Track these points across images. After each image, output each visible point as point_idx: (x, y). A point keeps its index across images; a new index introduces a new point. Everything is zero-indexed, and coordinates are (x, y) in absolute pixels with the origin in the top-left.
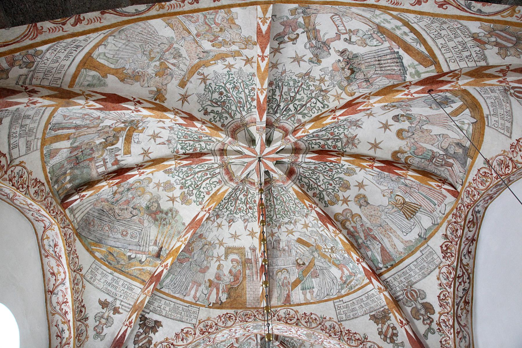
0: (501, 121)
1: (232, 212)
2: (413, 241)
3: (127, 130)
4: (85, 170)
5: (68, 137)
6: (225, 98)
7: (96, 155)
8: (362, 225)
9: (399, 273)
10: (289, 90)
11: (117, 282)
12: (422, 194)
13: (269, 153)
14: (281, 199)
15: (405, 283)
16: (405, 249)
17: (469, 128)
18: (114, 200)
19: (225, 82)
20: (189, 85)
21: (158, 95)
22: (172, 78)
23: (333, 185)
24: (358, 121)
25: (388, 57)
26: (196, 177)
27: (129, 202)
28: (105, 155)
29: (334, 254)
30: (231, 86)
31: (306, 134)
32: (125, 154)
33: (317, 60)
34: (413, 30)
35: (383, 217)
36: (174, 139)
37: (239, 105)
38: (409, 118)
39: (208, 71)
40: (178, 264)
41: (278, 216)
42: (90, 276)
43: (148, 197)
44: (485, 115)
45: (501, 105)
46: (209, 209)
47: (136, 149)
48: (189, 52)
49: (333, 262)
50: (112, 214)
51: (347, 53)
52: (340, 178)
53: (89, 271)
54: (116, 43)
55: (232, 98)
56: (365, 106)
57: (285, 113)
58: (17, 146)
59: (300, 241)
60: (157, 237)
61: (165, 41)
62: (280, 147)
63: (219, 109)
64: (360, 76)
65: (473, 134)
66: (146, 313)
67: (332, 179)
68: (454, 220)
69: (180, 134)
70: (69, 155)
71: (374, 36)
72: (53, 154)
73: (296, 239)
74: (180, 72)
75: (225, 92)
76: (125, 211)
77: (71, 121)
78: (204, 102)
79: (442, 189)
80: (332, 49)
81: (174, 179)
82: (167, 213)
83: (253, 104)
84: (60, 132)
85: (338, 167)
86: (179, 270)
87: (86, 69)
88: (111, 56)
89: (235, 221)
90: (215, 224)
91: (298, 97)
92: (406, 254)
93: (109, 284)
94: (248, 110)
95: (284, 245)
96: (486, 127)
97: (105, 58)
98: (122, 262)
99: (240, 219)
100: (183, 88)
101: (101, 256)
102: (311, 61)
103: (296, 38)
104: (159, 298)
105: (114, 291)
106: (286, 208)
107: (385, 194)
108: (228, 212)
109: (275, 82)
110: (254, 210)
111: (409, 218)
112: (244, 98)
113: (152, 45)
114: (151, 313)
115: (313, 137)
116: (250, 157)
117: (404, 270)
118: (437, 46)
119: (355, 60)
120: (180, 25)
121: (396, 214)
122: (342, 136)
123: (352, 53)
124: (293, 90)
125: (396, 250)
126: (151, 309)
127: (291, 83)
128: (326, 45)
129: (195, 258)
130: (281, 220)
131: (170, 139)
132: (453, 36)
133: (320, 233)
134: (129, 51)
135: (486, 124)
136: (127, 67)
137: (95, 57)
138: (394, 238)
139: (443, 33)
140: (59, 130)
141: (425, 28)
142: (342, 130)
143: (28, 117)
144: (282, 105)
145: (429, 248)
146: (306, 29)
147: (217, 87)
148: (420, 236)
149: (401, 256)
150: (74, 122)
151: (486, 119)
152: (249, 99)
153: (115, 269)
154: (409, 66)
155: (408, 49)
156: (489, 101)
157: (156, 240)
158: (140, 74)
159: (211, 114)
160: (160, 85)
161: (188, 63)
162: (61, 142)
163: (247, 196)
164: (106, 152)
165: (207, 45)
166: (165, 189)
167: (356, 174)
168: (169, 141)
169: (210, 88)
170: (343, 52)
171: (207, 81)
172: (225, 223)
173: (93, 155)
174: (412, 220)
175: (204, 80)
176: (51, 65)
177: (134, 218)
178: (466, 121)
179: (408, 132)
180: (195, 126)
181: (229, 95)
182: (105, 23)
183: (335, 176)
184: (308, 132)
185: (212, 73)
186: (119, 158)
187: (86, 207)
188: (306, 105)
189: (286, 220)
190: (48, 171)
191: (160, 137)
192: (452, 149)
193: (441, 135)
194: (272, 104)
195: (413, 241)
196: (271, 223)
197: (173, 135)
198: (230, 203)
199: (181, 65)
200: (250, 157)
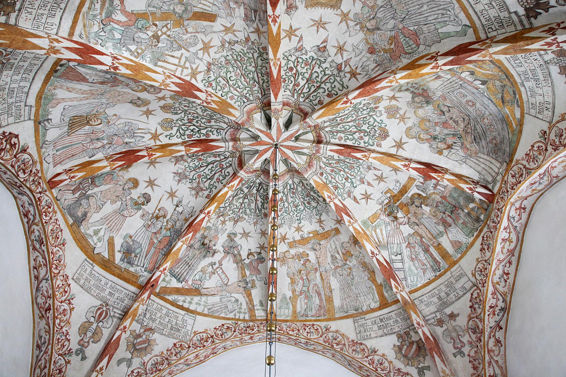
0: (85, 275)
1: (318, 62)
2: (50, 110)
3: (400, 202)
4: (455, 195)
5: (439, 247)
7: (438, 198)
8: (127, 85)
9: (36, 68)
10: (249, 205)
11: (525, 73)
12: (77, 144)
13: (266, 151)
14: (248, 80)
15: (16, 62)
16: (53, 95)
17: (93, 240)
18: (456, 140)
20: (334, 227)
22: (343, 243)
23: (182, 106)
24: (179, 181)
25: (185, 274)
26: (355, 117)
27: (444, 123)
28: (432, 191)
29: (150, 34)
30: (299, 207)
31: (230, 185)
32: (415, 180)
33: (231, 237)
34: (181, 308)
35: (104, 100)
38: (137, 205)
39: (315, 227)
40: (422, 37)
41: (251, 56)
42: (546, 112)
43: (420, 112)
44: (94, 264)
45: (97, 287)
46: (346, 102)
47: (403, 178)
49: (147, 19)
50: (469, 126)
51: (211, 255)
52: (176, 114)
53: (540, 116)
55: (300, 197)
56: (188, 238)
57: (251, 184)
58: (463, 287)
59: (211, 17)
60: (433, 80)
61: (338, 276)
62: (255, 161)
63: (312, 193)
64: (197, 245)
65: (86, 240)
66: (519, 17)
67: (186, 111)
68: (34, 171)
69: (356, 171)
70: (453, 225)
71: (199, 282)
72: (457, 245)
73: (219, 19)
76: (454, 117)
77: (425, 262)
79: (68, 178)
80: (222, 251)
81: (381, 118)
82: (407, 90)
83: (282, 194)
84: (439, 258)
85: (183, 127)
86: (425, 28)
88: (371, 294)
89: (316, 48)
90: (346, 56)
91: (241, 200)
92: (46, 90)
93: (537, 80)
94: (286, 186)
95: (237, 10)
96: (86, 257)
98: (498, 83)
99: (308, 49)
101: (516, 108)
102: (235, 234)
103: (249, 255)
104: (482, 18)
105: (538, 70)
106: (240, 65)
107: (115, 117)
108: (324, 66)
110: (285, 68)
111: (72, 118)
112: (289, 197)
114: (512, 10)
115: (219, 155)
116: (287, 147)
117: (32, 74)
118: (164, 307)
119: (204, 253)
121: (88, 110)
122: (189, 160)
123: (208, 257)
124: (246, 204)
125: (65, 88)
126: (506, 14)
127: (248, 211)
128: (227, 253)
129: (392, 23)
130: (245, 49)
131: (367, 170)
132: (162, 321)
133: (183, 51)
135: (88, 259)
136: (366, 278)
138: (77, 96)
139: (167, 319)
140: (437, 261)
141: (178, 315)
142: (191, 165)
143: (440, 298)
144: (254, 191)
145: (26, 119)
146: (243, 263)
148: (48, 120)
149: (51, 85)
150: (424, 258)
151: (92, 262)
152: (284, 198)
153: (514, 84)
154: (171, 280)
155: (178, 291)
156: (104, 280)
157: (436, 78)
161: (329, 246)
162: (445, 247)
163: (294, 85)
164: (429, 193)
165: (312, 256)
166: (398, 109)
167: (159, 124)
168: (369, 168)
170: (215, 253)
172: (332, 51)
173: (440, 199)
174: (69, 119)
175: (320, 221)
176: (400, 321)
177: (449, 105)
178: (99, 245)
179: (129, 188)
180: (336, 205)
181: (302, 200)
182: (351, 359)
183: (183, 115)
184: (228, 188)
185: (313, 224)
186: (422, 180)
187: (484, 161)
188: (233, 198)
189: (238, 47)
190: (472, 238)
191: (376, 175)
192: (85, 204)
193: (101, 206)
195: (50, 110)
196: (261, 50)
198: (319, 80)
200: (287, 147)
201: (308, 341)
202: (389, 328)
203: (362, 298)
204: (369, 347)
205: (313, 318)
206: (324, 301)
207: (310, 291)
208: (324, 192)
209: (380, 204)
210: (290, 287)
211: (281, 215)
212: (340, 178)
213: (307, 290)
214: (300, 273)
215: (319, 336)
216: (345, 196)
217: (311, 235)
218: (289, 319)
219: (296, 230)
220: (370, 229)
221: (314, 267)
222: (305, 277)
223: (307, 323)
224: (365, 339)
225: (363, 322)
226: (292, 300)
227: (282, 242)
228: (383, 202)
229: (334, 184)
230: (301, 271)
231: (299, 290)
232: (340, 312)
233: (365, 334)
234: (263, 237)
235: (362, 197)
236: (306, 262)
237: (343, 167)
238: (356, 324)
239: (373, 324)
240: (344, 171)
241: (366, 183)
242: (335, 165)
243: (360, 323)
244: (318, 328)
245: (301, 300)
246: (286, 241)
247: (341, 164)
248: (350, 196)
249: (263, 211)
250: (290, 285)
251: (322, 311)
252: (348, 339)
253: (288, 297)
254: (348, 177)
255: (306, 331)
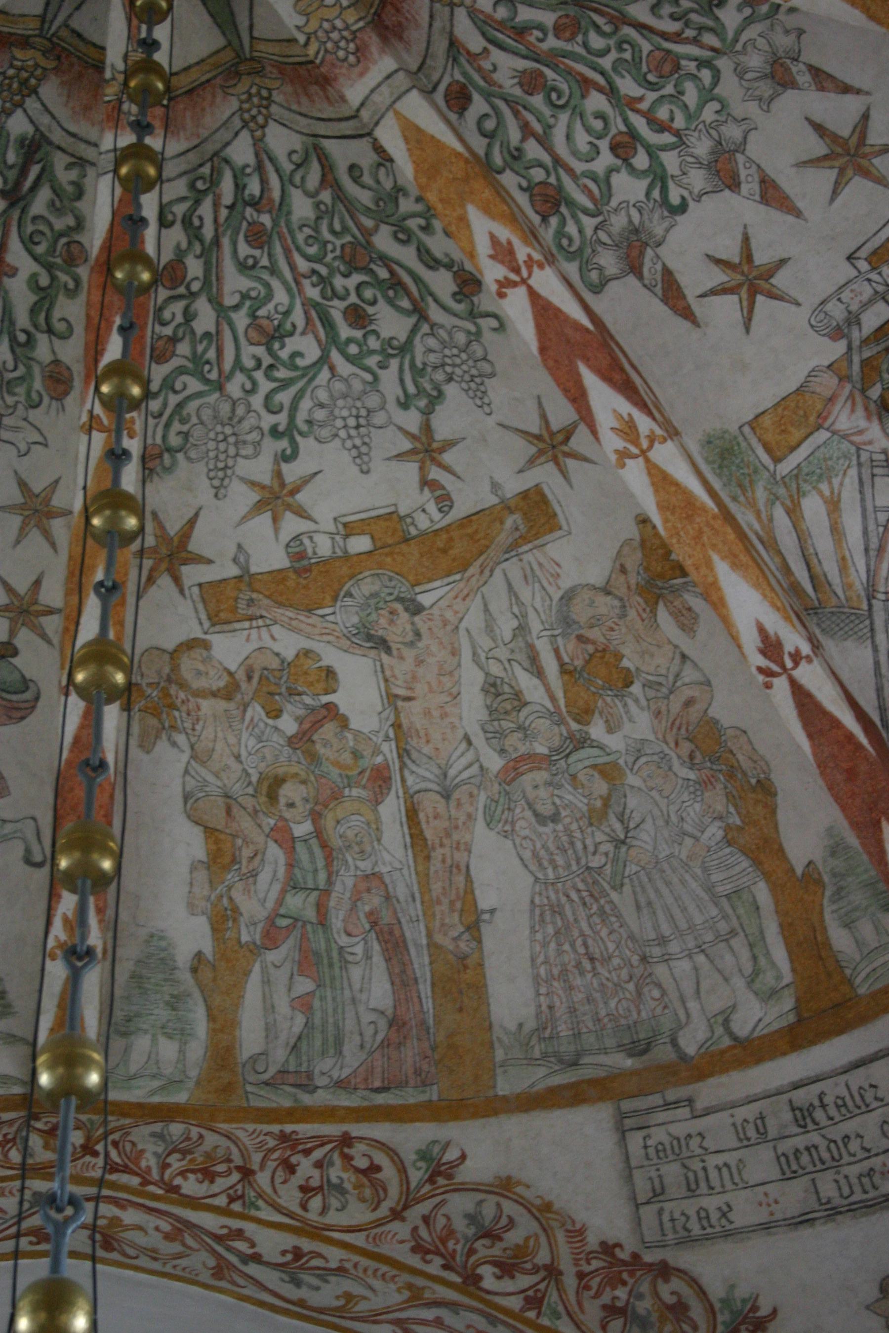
6: (339, 282)
19: (325, 374)
20: (513, 486)
21: (661, 576)
22: (568, 597)
30: (293, 344)
36: (740, 72)
37: (266, 219)
48: (447, 682)
54: (688, 988)
55: (303, 265)
61: (525, 823)
63: (384, 241)
69: (691, 96)
74: (525, 594)
75: (337, 316)
78: (461, 338)
83: (176, 235)
87: (850, 982)
88: (738, 943)
94: (214, 181)
97: (762, 961)
100: (538, 490)
109: (38, 385)
112: (229, 267)
113: (579, 846)
120: (436, 887)
131: (765, 88)
134: (670, 900)
136: (715, 831)
137: (788, 1003)
147: (372, 361)
152: (194, 267)
158: (686, 747)
159: (439, 255)
160: (632, 614)
161: (474, 619)
169: (412, 389)
171: (414, 429)
181: (313, 293)
185: (378, 465)
191: (819, 129)
194: (59, 224)
197: (738, 110)
199: (508, 636)
201: (306, 1245)
202: (853, 1171)
203: (683, 966)
204: (716, 1291)
205: (345, 1101)
206: (425, 989)
207: (337, 922)
208: (473, 213)
209: (837, 333)
210: (202, 890)
211: (168, 384)
212: (582, 139)
213: (310, 914)
214: (273, 797)
215: (384, 1211)
216: (609, 261)
217: (360, 544)
218: (181, 1097)
219: (259, 507)
220: (761, 495)
221: (365, 763)
222: (302, 829)
223: (305, 1129)
224: (687, 1241)
225: (679, 1130)
226: (206, 974)
227: (165, 581)
228: (853, 319)
229: (538, 175)
230: (279, 781)
231: (262, 914)
232: (531, 1061)
233: (691, 1207)
234: (35, 536)
235: (719, 277)
236: (317, 724)
237: (606, 62)
238: (635, 1141)
239: (745, 1143)
240: (611, 92)
241: (750, 186)
242: (552, 42)
243: (659, 1135)
244: (380, 1158)
245: (266, 982)
246: (192, 574)
247: (597, 42)
248: (635, 268)
249: (43, 350)
250: (202, 875)
251: (410, 1054)
252: (577, 1233)
253: (183, 956)
254: (633, 134)
255: (298, 1179)
